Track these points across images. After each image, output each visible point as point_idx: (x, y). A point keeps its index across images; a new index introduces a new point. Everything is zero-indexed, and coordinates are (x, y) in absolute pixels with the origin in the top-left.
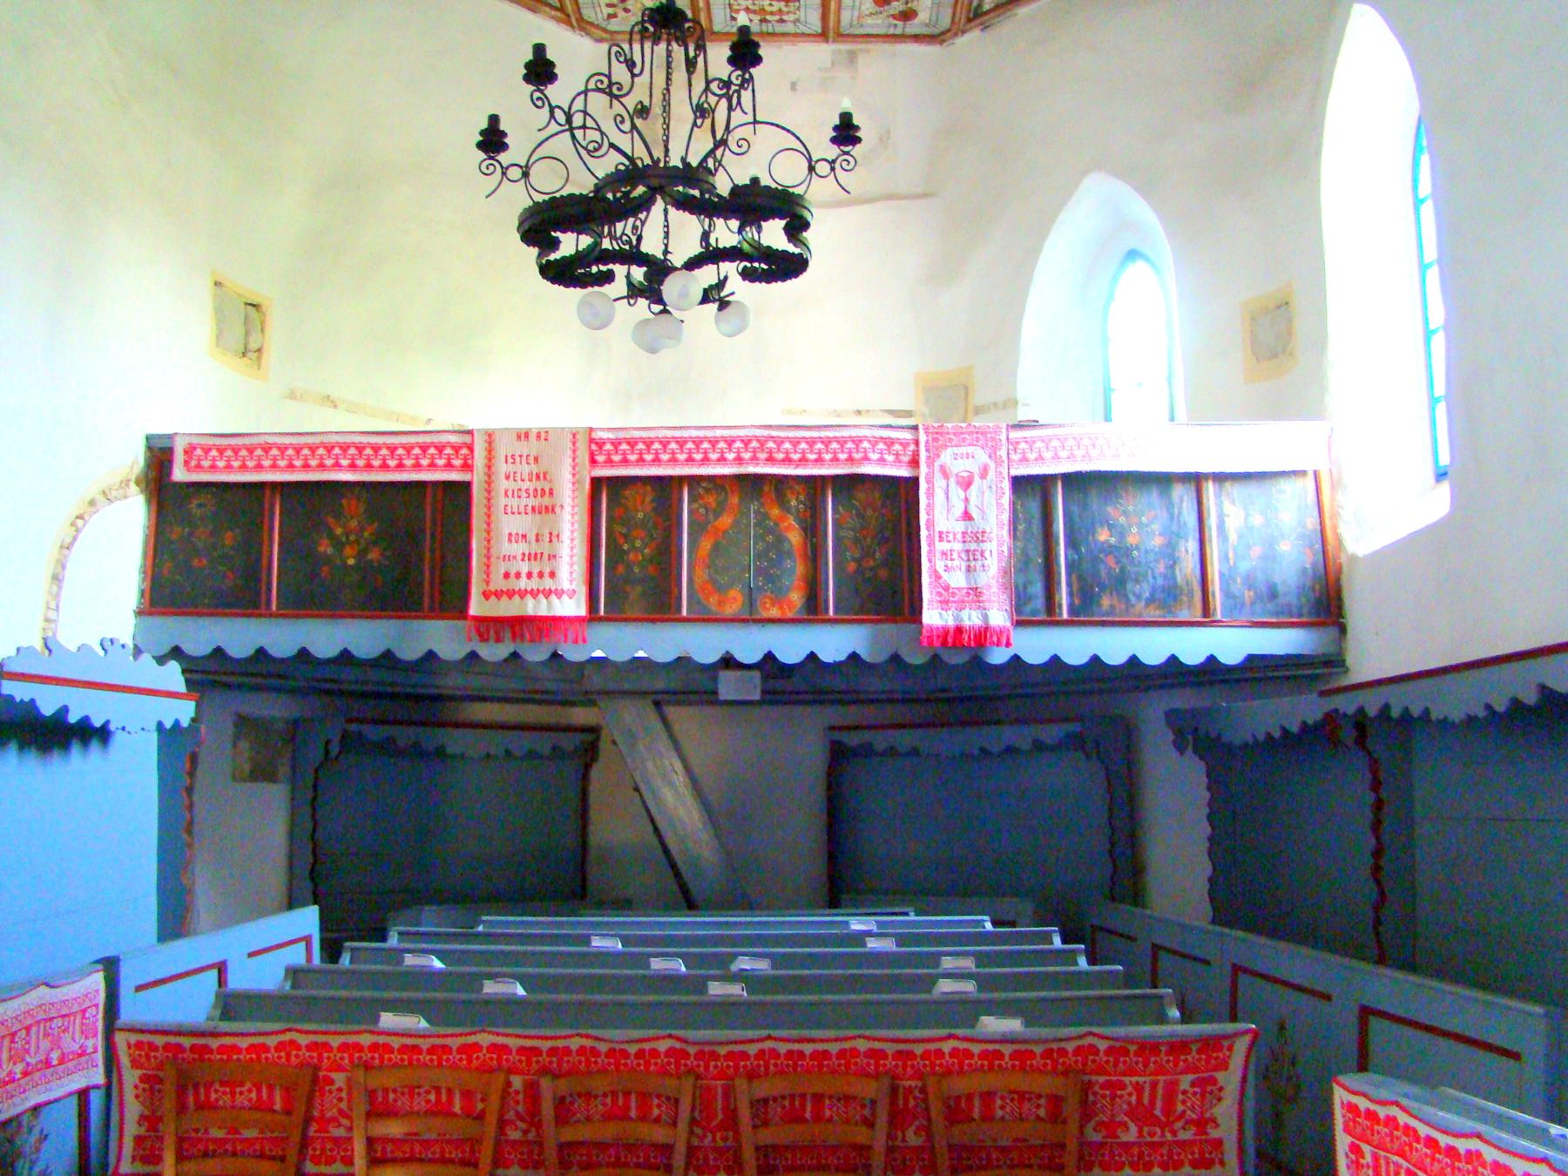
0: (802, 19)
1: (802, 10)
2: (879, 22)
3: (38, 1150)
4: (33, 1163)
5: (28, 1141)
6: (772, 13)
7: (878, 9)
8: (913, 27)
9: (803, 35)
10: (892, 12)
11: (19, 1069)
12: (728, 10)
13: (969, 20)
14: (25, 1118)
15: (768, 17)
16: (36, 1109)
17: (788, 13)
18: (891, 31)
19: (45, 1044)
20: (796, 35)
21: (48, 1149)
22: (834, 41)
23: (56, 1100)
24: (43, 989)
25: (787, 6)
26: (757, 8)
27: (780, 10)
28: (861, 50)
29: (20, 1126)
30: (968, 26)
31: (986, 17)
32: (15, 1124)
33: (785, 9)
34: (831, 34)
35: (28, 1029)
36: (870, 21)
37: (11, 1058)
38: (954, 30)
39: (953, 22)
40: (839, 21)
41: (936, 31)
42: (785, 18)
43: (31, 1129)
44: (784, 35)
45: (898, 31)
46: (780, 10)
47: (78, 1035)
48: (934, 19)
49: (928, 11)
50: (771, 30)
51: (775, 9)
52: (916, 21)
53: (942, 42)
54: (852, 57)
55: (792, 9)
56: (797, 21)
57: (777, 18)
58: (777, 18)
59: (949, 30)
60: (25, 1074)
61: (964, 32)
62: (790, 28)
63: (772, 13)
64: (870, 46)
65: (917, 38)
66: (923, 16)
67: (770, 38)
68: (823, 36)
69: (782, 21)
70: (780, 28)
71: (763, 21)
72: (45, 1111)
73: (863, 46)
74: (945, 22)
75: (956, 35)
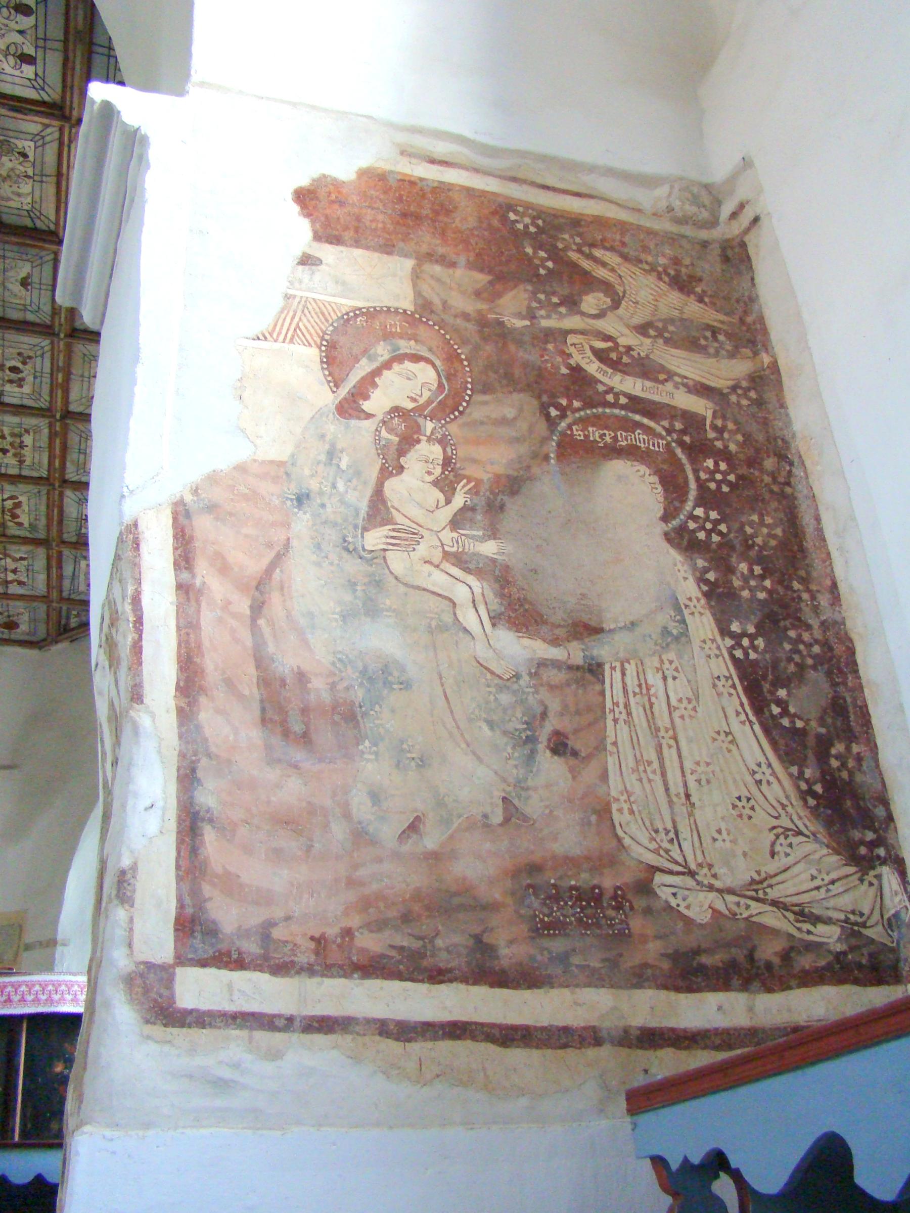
8: (17, 634)
13: (60, 634)
31: (74, 632)
38: (49, 639)
39: (48, 634)
49: (27, 624)
52: (18, 630)
53: (40, 648)
61: (57, 642)
66: (24, 627)
75: (51, 643)
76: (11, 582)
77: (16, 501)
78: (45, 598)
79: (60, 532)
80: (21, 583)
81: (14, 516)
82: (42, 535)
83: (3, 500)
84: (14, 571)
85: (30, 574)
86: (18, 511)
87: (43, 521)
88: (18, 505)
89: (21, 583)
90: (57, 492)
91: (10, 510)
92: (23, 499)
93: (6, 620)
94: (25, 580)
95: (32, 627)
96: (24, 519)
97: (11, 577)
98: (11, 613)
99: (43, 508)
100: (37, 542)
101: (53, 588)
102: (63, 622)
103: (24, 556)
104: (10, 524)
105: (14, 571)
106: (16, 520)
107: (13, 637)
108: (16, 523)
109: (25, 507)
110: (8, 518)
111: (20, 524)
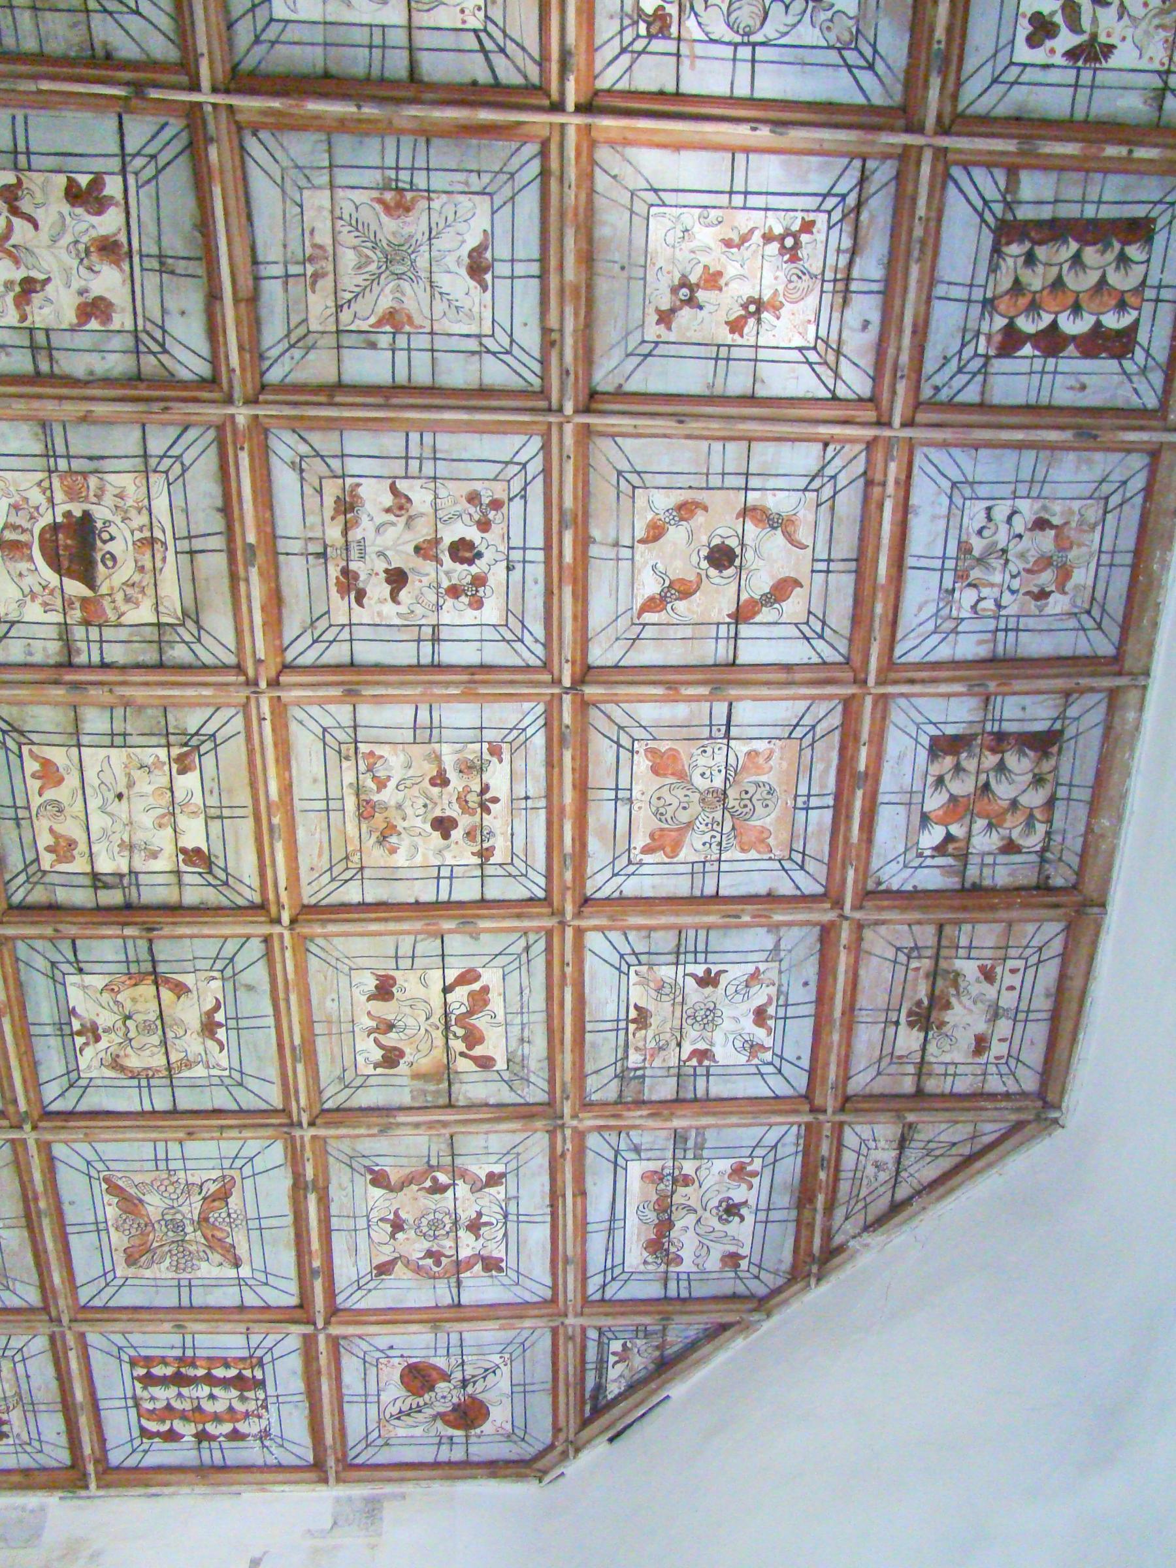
0: (275, 1431)
1: (272, 1408)
2: (418, 1431)
6: (217, 1418)
7: (413, 1401)
9: (280, 1468)
10: (441, 1407)
12: (133, 1412)
13: (585, 1423)
15: (211, 1428)
17: (247, 1415)
18: (444, 1454)
20: (266, 1468)
22: (339, 1480)
25: (243, 1399)
26: (187, 1406)
27: (231, 1409)
28: (394, 1496)
30: (586, 1433)
33: (239, 1407)
34: (331, 1462)
36: (401, 1430)
39: (556, 1429)
40: (342, 1431)
41: (527, 1451)
42: (242, 1427)
44: (248, 1468)
45: (458, 1454)
46: (231, 1409)
48: (520, 1423)
50: (218, 1460)
51: (220, 1407)
52: (487, 1427)
53: (541, 1475)
54: (372, 1509)
55: (251, 1406)
56: (265, 1435)
57: (227, 1428)
58: (227, 1428)
59: (552, 1447)
62: (251, 1453)
63: (217, 1418)
64: (408, 1488)
65: (494, 1468)
66: (499, 1416)
67: (221, 1477)
68: (317, 1470)
69: (235, 1435)
70: (236, 1454)
71: (202, 1436)
73: (389, 1489)
74: (542, 1432)
75: (564, 1455)
76: (469, 1264)
77: (476, 986)
78: (551, 1304)
79: (581, 1077)
80: (491, 1265)
81: (473, 1038)
82: (536, 1093)
83: (446, 990)
84: (475, 1227)
85: (512, 1226)
86: (480, 1021)
87: (538, 1048)
88: (480, 1000)
89: (491, 1265)
90: (569, 933)
91: (460, 1020)
92: (490, 977)
93: (457, 1397)
94: (499, 1253)
95: (519, 1410)
96: (494, 1046)
97: (468, 1246)
98: (469, 1371)
99: (538, 1001)
100: (524, 1113)
101: (566, 1261)
102: (590, 1382)
103: (498, 1169)
104: (463, 1064)
105: (475, 1227)
106: (478, 1051)
107: (481, 1451)
108: (474, 1059)
109: (496, 1003)
110: (458, 1045)
111: (485, 1063)
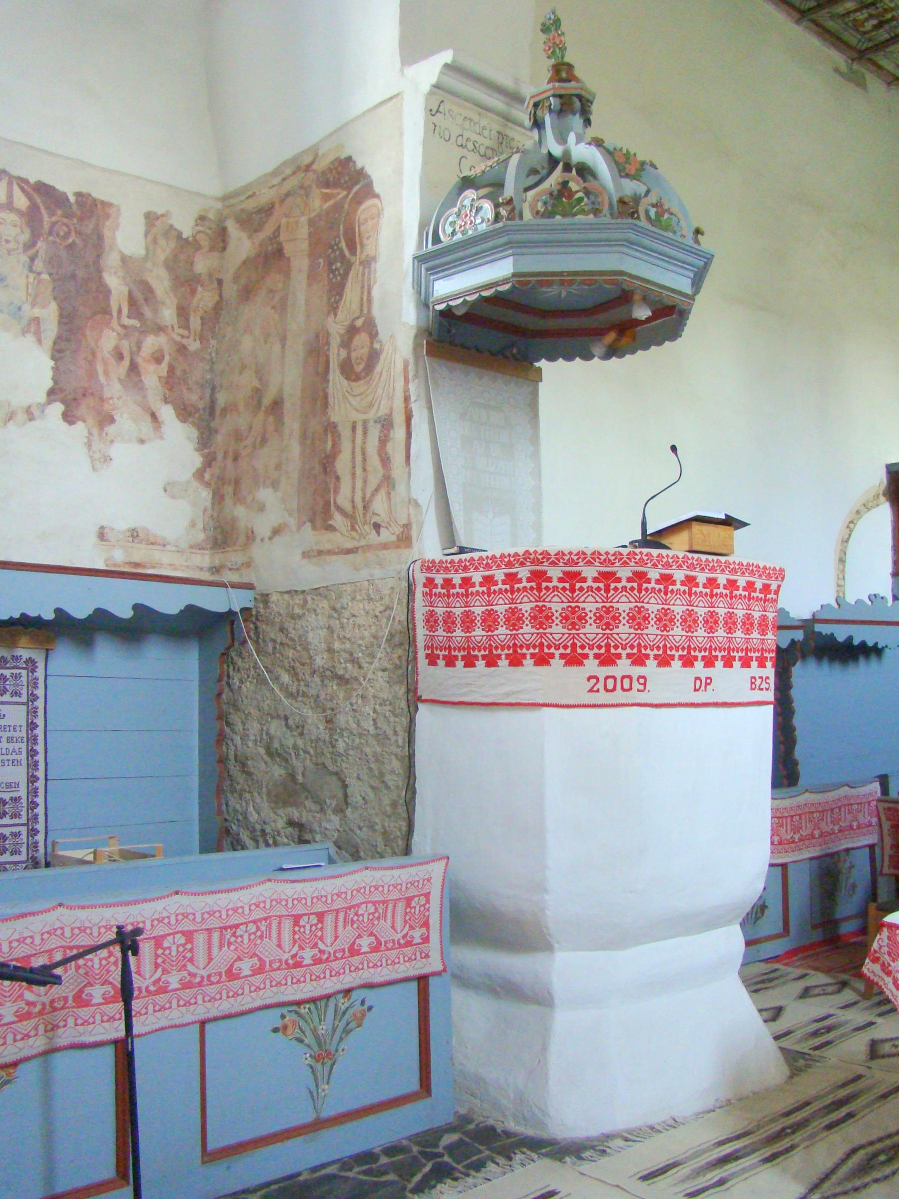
3: (850, 872)
4: (847, 878)
5: (844, 867)
11: (836, 828)
14: (843, 855)
16: (847, 850)
19: (849, 817)
21: (854, 872)
23: (858, 848)
24: (846, 788)
29: (839, 857)
32: (836, 856)
35: (840, 808)
37: (832, 822)
43: (845, 861)
47: (866, 813)
60: (840, 831)
72: (852, 852)
